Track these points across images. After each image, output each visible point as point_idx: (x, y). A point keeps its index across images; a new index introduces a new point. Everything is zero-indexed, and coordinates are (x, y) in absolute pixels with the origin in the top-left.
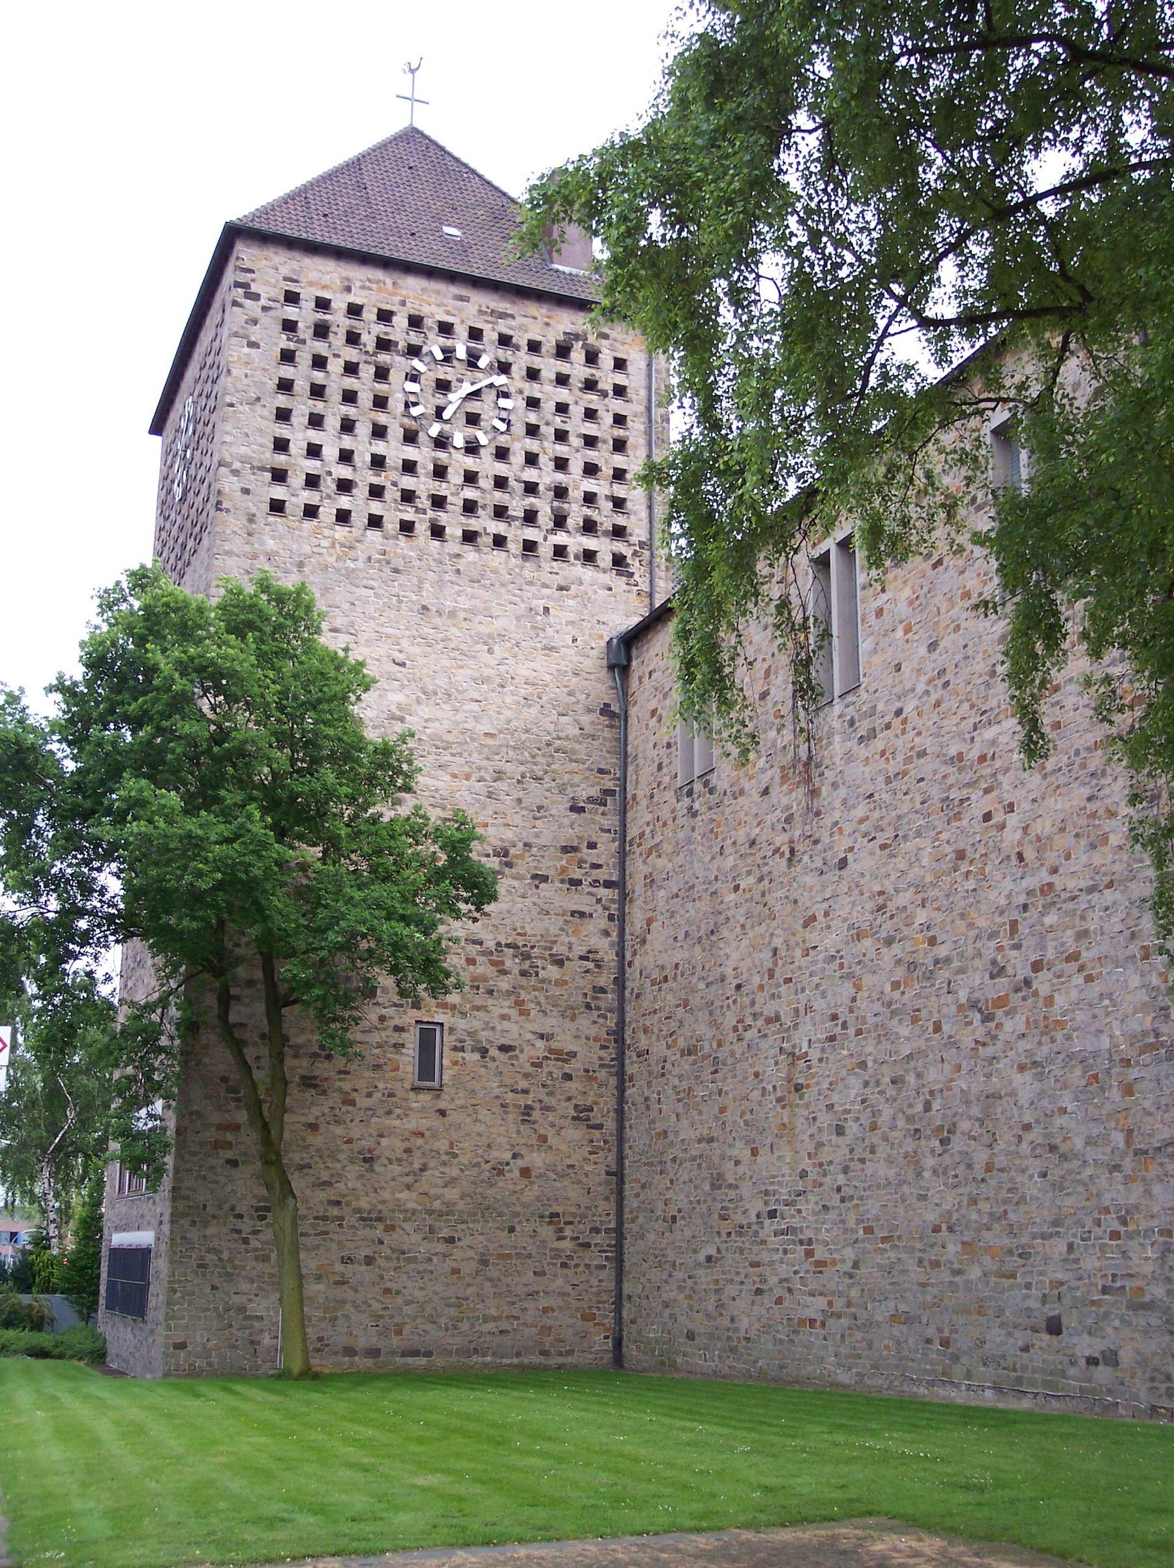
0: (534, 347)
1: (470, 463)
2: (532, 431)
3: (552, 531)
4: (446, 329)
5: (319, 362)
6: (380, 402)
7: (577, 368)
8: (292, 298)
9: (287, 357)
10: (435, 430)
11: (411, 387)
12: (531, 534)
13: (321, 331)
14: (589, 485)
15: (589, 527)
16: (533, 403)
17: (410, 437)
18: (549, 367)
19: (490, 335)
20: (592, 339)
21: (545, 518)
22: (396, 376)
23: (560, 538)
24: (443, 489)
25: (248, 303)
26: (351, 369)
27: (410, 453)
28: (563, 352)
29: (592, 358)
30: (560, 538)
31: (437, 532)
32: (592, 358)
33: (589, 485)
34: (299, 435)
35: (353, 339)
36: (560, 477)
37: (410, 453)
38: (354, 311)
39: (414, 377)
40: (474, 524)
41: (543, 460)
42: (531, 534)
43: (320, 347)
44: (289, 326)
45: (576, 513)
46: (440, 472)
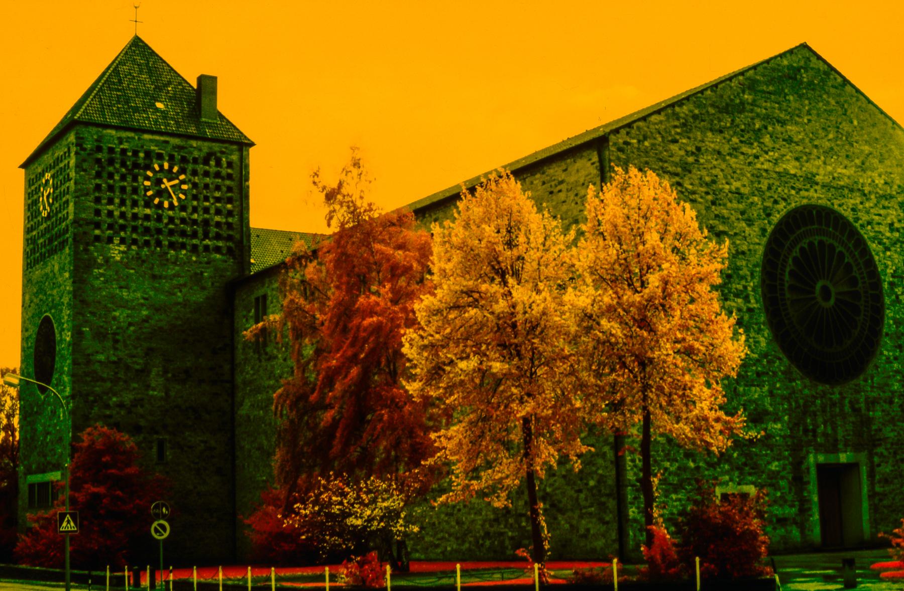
0: (195, 161)
1: (171, 213)
2: (195, 197)
3: (203, 240)
4: (160, 157)
5: (111, 176)
6: (135, 191)
7: (212, 168)
8: (99, 149)
9: (98, 175)
10: (156, 201)
11: (147, 183)
12: (195, 241)
13: (111, 162)
14: (218, 218)
15: (218, 237)
16: (195, 185)
17: (147, 205)
18: (200, 168)
19: (178, 157)
20: (219, 155)
21: (200, 235)
22: (140, 179)
23: (207, 242)
24: (161, 226)
25: (82, 152)
26: (123, 178)
27: (148, 211)
28: (206, 162)
29: (218, 163)
30: (207, 242)
31: (159, 243)
32: (218, 163)
33: (218, 218)
34: (105, 208)
35: (123, 164)
36: (206, 216)
37: (148, 211)
38: (124, 151)
39: (147, 178)
40: (173, 239)
41: (199, 209)
42: (195, 241)
43: (111, 169)
44: (98, 161)
45: (213, 230)
46: (159, 219)
